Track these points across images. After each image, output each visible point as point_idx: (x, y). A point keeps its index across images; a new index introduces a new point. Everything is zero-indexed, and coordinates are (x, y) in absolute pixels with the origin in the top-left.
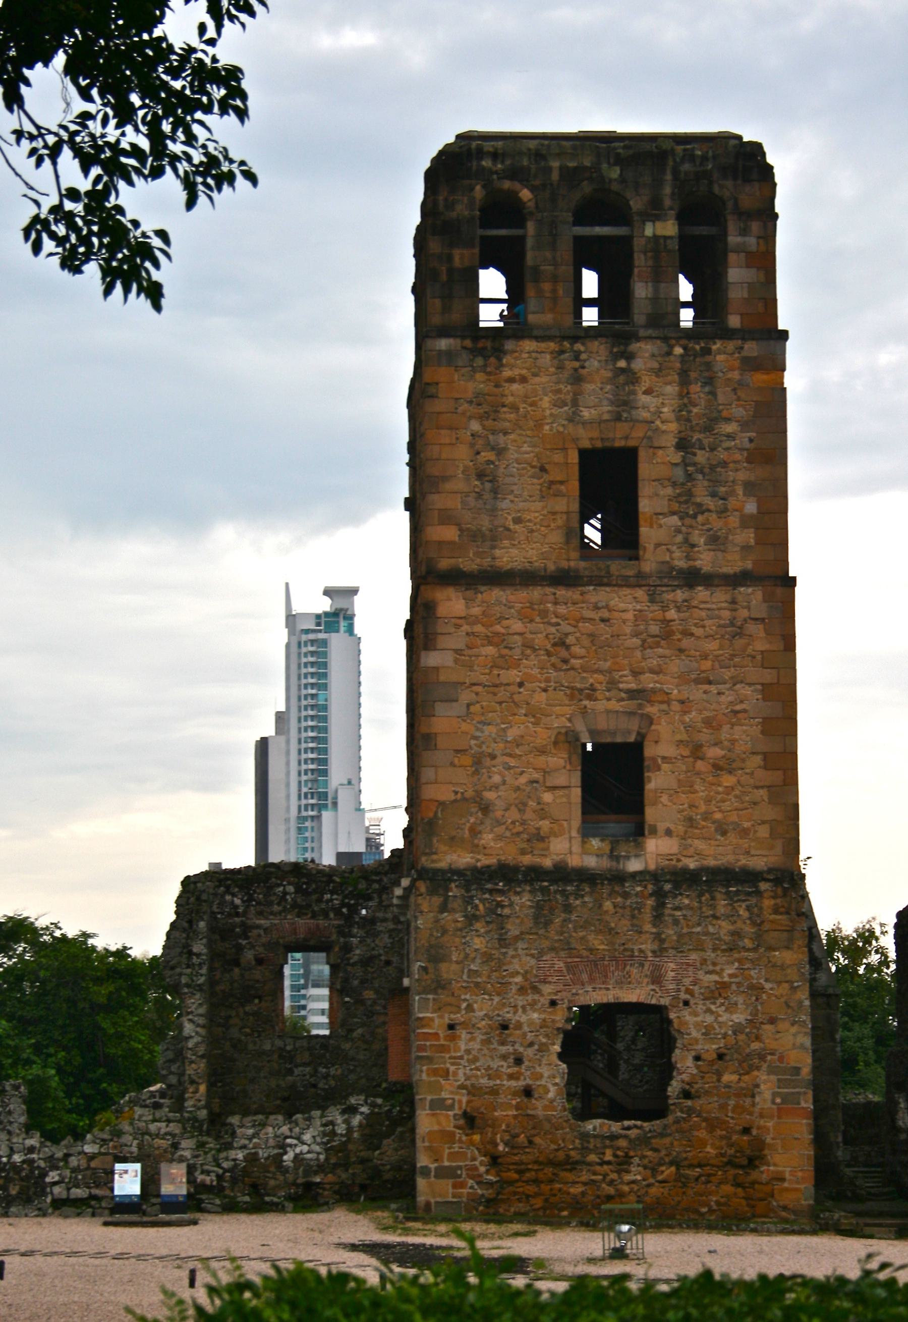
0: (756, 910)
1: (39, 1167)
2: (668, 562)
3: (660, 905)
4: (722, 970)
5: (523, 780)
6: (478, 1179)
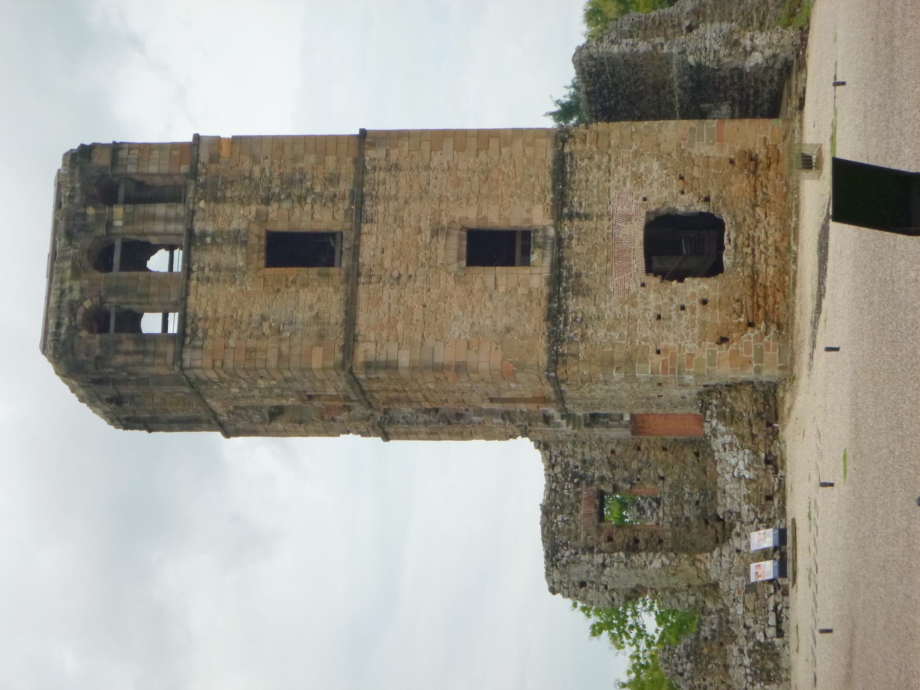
0: (583, 155)
1: (754, 646)
2: (346, 211)
3: (578, 215)
4: (623, 176)
5: (489, 305)
6: (764, 335)
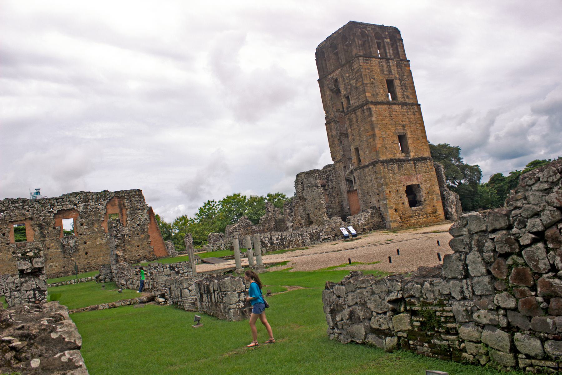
3: (415, 165)
5: (390, 142)
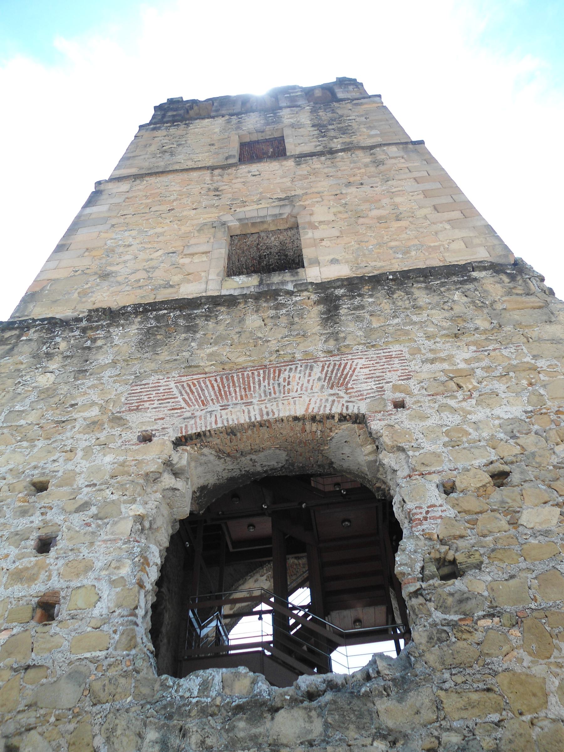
4: (452, 356)
